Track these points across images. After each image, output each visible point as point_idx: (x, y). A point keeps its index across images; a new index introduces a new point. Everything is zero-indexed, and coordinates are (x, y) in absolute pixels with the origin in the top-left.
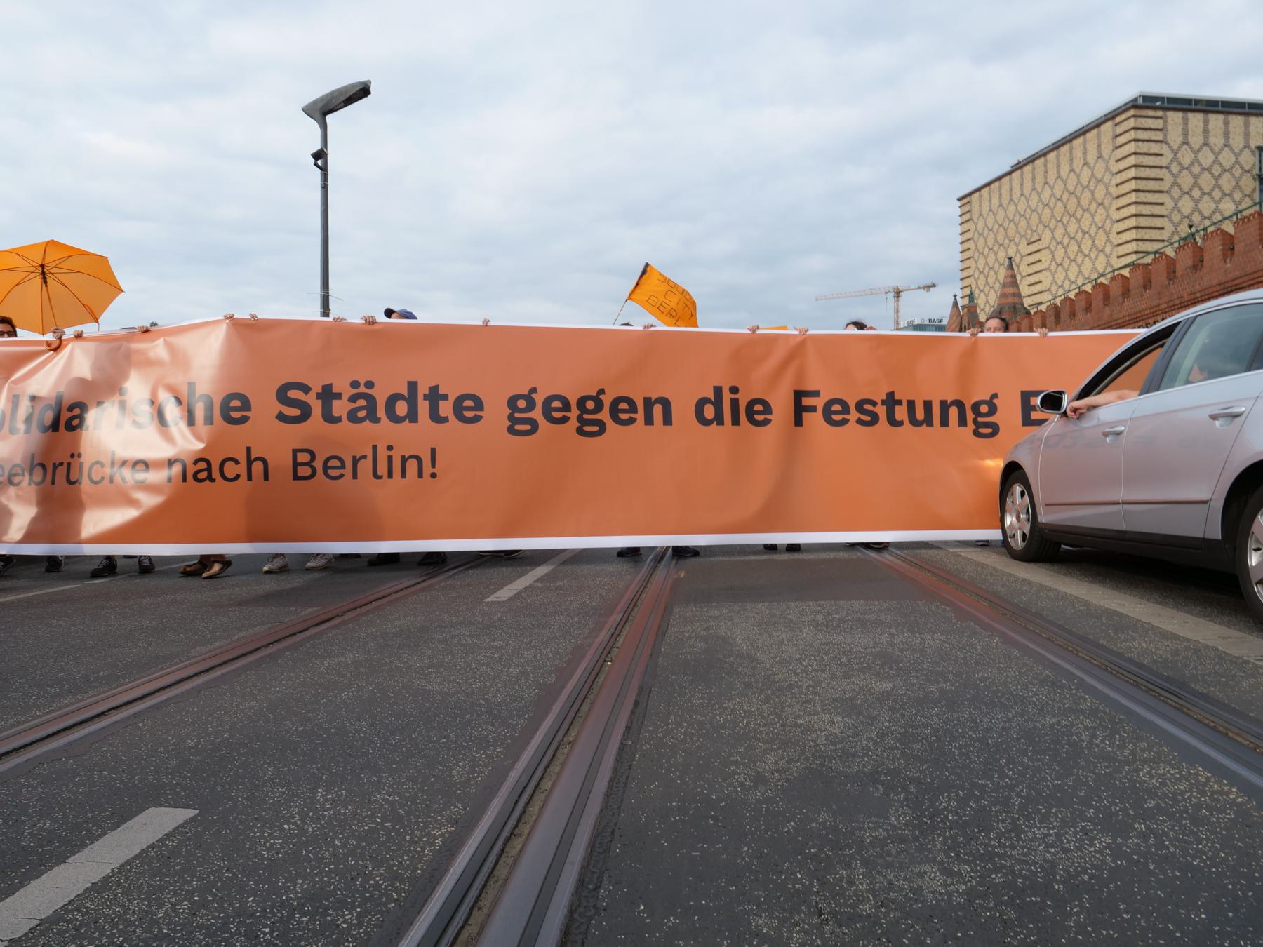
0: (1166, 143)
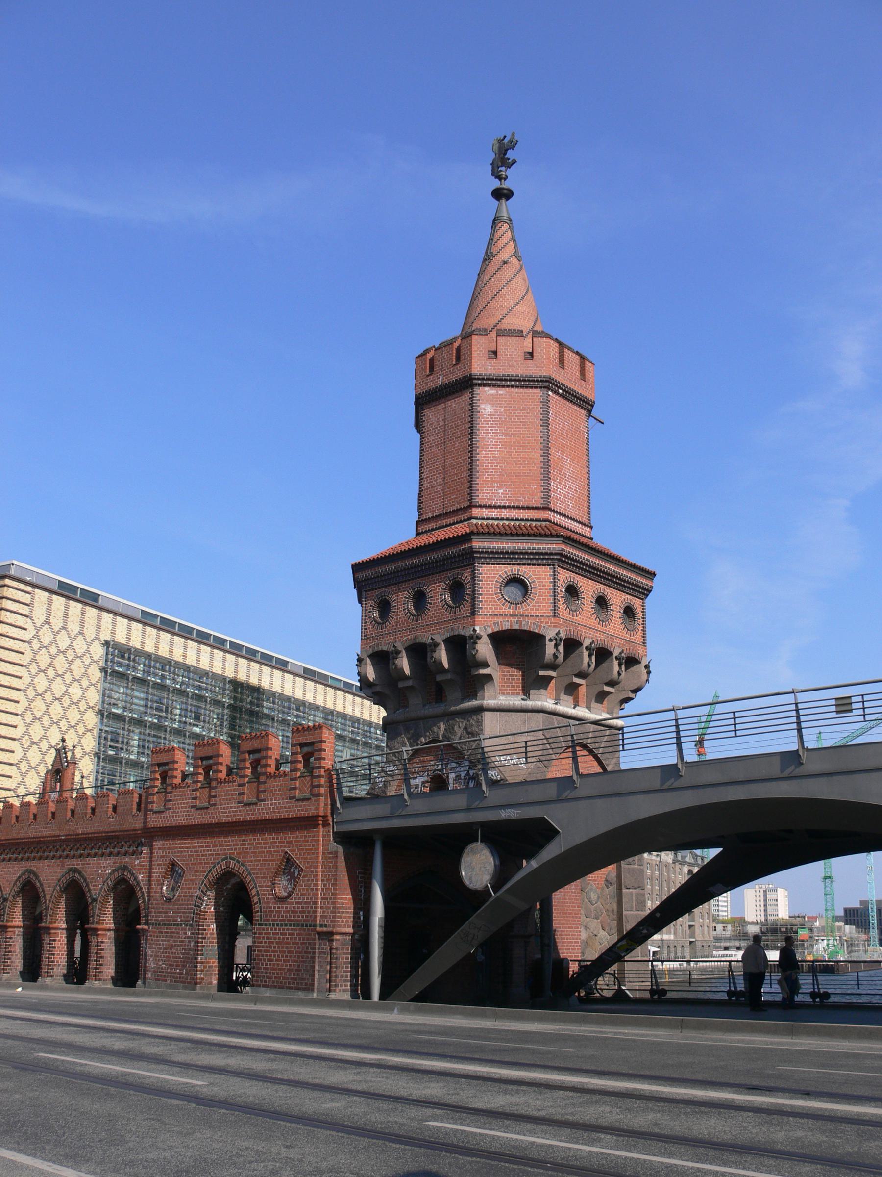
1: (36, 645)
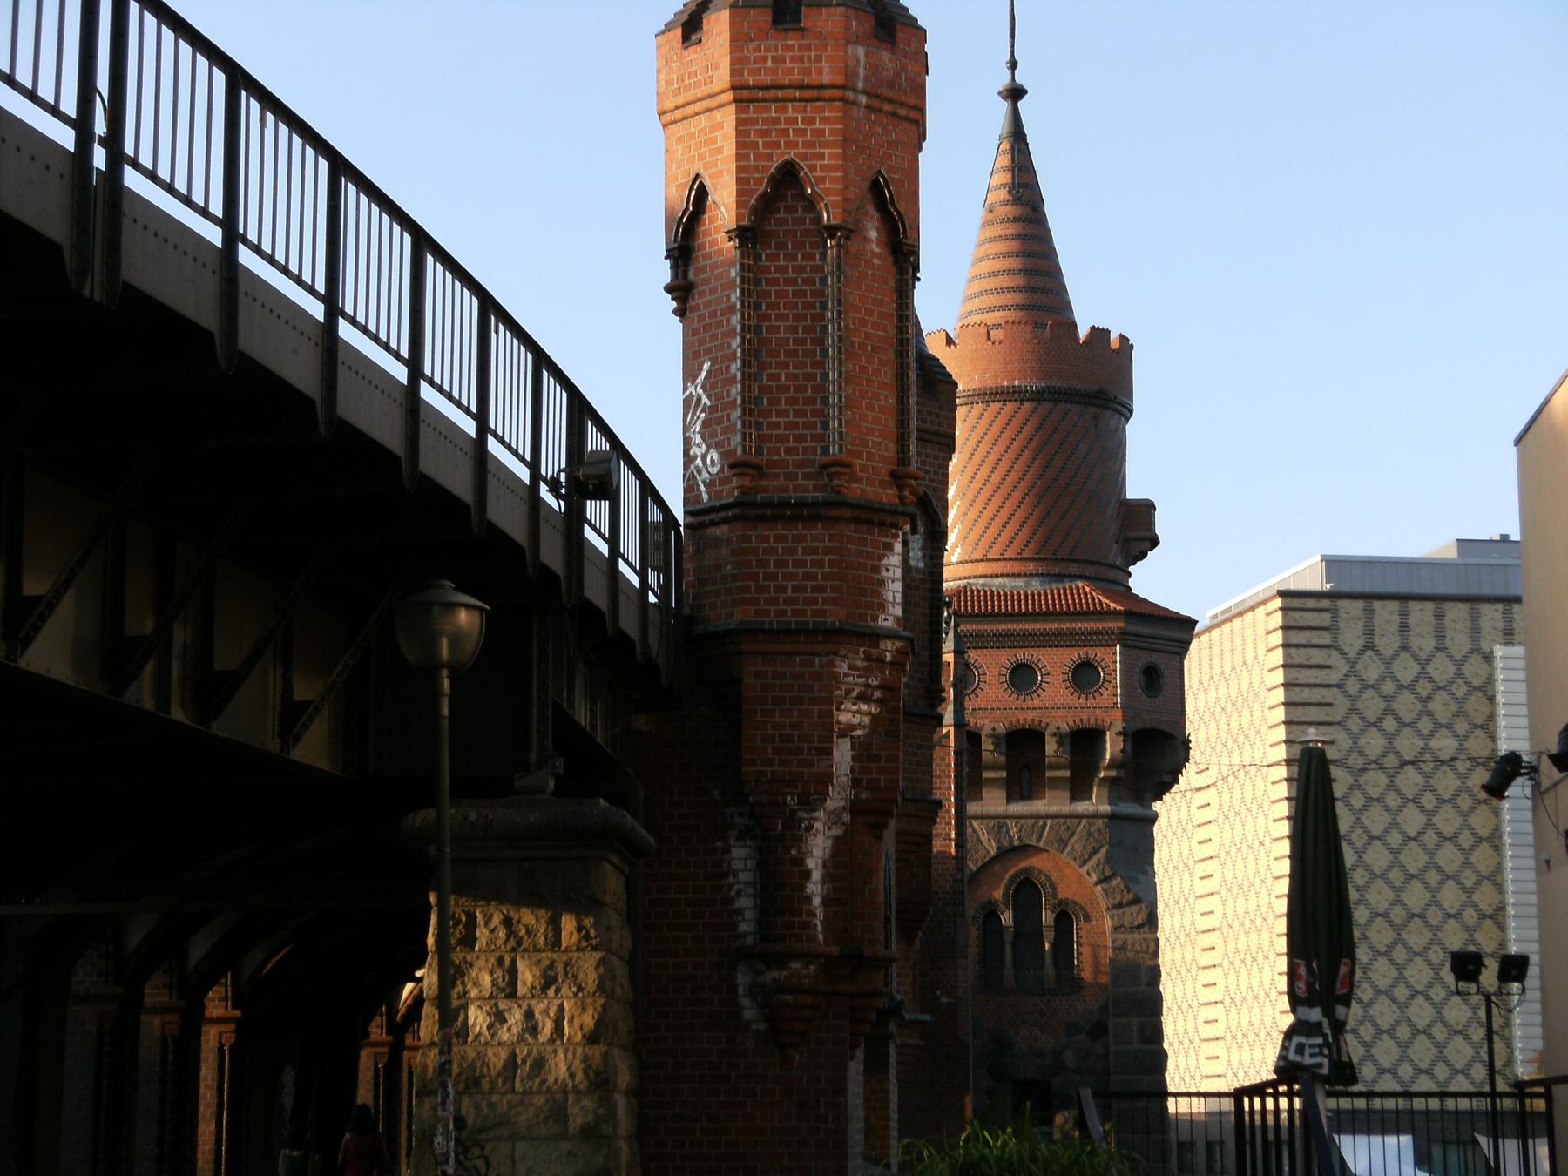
0: (1337, 648)
1: (1352, 686)
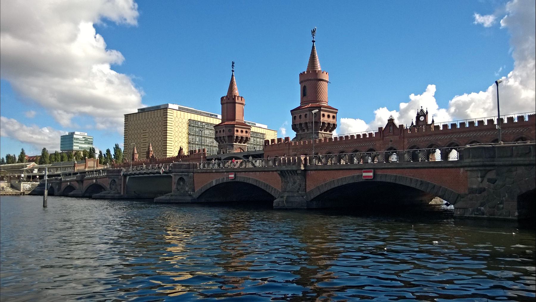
1: (175, 122)
